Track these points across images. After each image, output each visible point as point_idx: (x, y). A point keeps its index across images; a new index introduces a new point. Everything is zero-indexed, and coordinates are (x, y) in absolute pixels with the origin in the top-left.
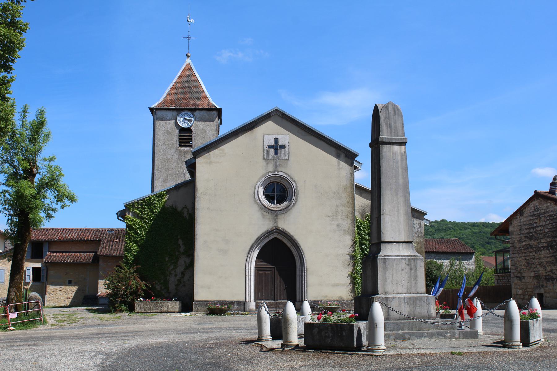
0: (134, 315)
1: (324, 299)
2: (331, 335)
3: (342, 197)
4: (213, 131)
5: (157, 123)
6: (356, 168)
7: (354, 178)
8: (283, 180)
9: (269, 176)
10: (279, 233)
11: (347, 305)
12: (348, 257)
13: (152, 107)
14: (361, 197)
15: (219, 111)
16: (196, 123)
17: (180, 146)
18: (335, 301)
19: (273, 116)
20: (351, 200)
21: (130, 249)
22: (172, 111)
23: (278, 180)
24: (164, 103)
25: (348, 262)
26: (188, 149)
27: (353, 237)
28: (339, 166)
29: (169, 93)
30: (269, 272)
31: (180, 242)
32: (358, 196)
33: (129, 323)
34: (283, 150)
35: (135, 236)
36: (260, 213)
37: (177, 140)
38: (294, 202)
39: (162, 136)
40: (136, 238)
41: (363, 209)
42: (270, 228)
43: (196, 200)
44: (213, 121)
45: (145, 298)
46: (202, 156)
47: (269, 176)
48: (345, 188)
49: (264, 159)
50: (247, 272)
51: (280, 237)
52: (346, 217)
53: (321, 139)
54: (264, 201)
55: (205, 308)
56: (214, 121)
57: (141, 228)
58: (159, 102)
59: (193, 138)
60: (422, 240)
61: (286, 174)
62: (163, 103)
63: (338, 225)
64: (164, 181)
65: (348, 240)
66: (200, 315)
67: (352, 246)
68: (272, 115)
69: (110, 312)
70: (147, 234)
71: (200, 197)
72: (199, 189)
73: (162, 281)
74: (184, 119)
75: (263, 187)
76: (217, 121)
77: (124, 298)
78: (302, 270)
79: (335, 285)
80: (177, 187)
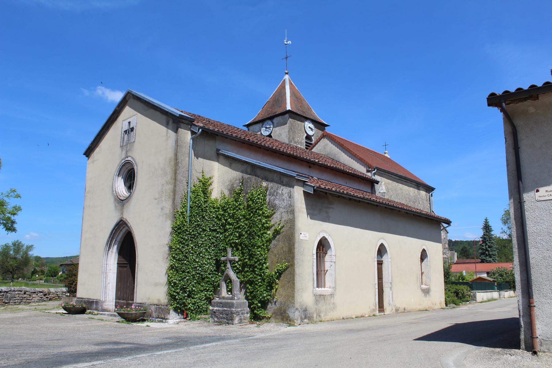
1: (148, 302)
3: (167, 173)
4: (286, 133)
9: (122, 163)
11: (163, 310)
12: (167, 248)
18: (154, 305)
19: (129, 99)
20: (173, 175)
25: (167, 255)
27: (172, 221)
28: (167, 135)
32: (227, 168)
34: (132, 133)
41: (232, 183)
46: (90, 157)
47: (122, 163)
49: (121, 146)
52: (169, 197)
54: (120, 191)
56: (286, 124)
61: (132, 158)
63: (162, 209)
65: (168, 227)
67: (171, 234)
71: (86, 196)
75: (121, 176)
79: (156, 285)
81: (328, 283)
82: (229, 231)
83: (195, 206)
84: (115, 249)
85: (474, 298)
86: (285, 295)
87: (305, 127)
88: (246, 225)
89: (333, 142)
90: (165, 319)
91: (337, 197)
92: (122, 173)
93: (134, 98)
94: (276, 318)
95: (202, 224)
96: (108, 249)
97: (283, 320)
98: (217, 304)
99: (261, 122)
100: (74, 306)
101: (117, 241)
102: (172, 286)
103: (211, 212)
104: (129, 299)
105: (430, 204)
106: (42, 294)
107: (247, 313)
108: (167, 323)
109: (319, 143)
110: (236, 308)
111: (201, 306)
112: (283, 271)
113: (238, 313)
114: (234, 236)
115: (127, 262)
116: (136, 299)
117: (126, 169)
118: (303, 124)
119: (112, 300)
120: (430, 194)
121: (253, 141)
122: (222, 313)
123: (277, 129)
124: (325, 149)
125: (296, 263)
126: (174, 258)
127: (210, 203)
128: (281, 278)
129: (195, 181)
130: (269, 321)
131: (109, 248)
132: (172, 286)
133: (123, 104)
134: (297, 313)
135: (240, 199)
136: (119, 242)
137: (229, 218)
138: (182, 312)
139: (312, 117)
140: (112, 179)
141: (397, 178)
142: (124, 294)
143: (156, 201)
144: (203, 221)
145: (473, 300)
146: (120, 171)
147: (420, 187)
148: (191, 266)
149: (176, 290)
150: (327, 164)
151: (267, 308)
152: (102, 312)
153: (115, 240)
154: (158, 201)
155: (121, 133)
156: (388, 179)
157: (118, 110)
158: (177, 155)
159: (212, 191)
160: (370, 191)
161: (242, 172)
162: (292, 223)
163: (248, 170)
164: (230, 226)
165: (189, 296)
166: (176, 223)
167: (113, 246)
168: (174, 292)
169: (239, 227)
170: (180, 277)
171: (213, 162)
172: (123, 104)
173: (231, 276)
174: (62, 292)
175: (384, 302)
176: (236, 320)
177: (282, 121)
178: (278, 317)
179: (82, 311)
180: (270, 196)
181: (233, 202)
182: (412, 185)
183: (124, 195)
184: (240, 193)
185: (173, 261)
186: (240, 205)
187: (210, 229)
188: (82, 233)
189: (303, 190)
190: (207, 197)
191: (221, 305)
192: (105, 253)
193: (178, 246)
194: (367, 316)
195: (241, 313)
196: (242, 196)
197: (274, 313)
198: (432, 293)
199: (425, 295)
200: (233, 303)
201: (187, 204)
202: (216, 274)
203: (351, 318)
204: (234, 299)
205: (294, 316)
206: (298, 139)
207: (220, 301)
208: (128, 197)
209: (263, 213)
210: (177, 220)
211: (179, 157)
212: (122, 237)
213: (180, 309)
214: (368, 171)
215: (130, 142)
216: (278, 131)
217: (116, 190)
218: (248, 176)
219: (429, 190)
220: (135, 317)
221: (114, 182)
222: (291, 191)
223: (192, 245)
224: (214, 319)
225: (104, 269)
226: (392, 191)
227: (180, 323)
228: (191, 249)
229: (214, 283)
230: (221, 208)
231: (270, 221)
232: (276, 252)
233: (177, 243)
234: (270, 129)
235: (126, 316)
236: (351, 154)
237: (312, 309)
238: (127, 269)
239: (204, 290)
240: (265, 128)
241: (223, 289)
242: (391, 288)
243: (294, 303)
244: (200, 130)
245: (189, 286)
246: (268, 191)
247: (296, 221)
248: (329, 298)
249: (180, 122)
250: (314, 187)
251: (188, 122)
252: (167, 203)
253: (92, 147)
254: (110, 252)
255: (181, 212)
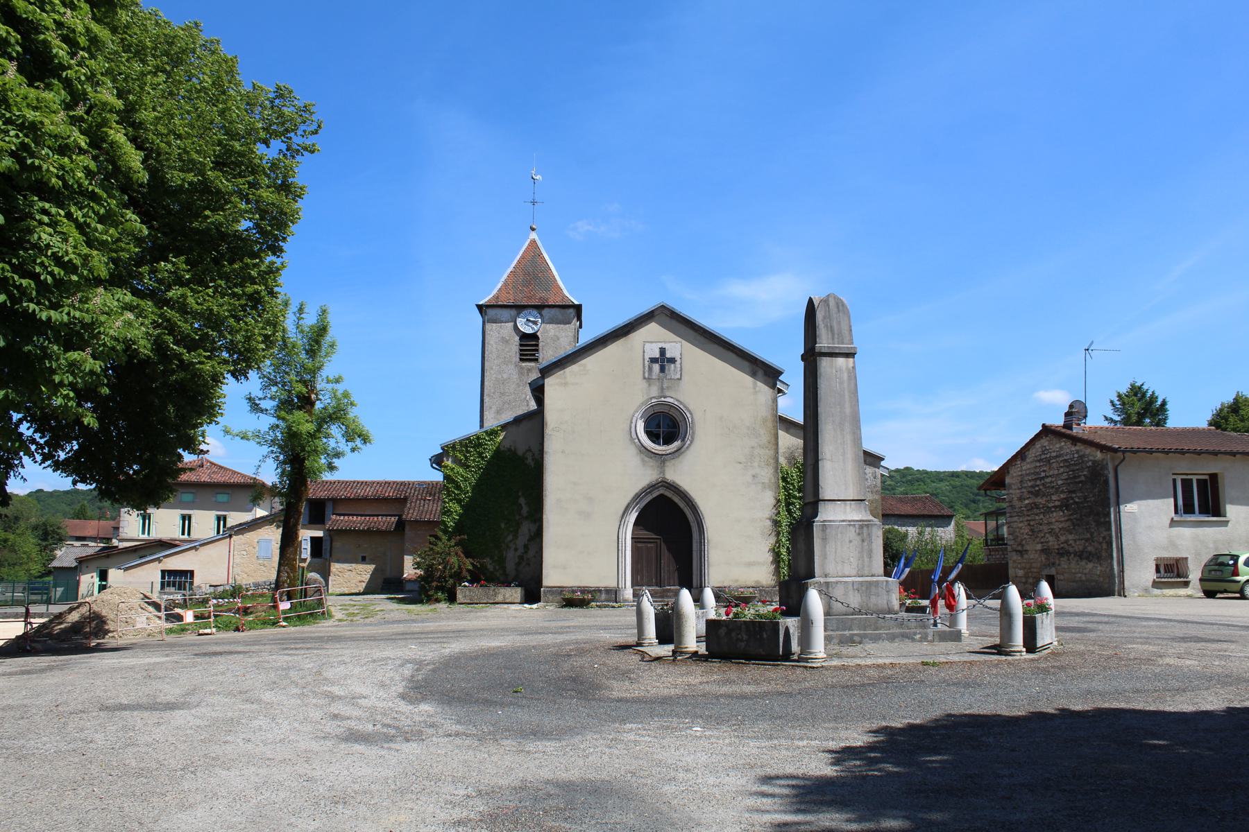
0: (455, 607)
1: (734, 585)
2: (745, 637)
5: (488, 326)
6: (780, 391)
7: (777, 405)
8: (672, 410)
10: (667, 488)
11: (767, 593)
12: (769, 523)
13: (481, 303)
15: (578, 309)
17: (521, 360)
21: (449, 511)
23: (666, 410)
24: (497, 298)
26: (532, 364)
28: (755, 388)
29: (506, 284)
30: (652, 545)
31: (522, 501)
33: (449, 619)
34: (673, 365)
35: (456, 492)
37: (518, 351)
38: (689, 442)
39: (494, 346)
40: (458, 495)
42: (654, 479)
43: (545, 439)
44: (569, 323)
45: (472, 582)
48: (764, 421)
49: (644, 378)
50: (620, 545)
51: (668, 494)
53: (729, 349)
55: (559, 598)
57: (466, 481)
58: (491, 296)
59: (540, 347)
60: (877, 497)
61: (677, 400)
62: (497, 297)
63: (754, 476)
64: (498, 412)
65: (769, 498)
66: (551, 608)
68: (656, 313)
69: (421, 602)
70: (474, 488)
72: (549, 424)
73: (496, 558)
74: (527, 320)
76: (576, 323)
77: (441, 582)
78: (701, 542)
79: (750, 564)
80: (518, 420)
84: (633, 517)
140: (629, 422)
177: (560, 317)
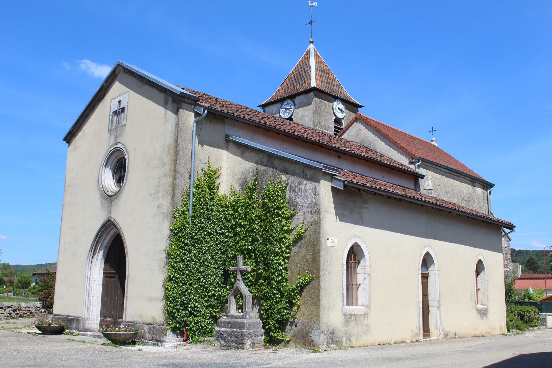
1: (140, 320)
3: (165, 163)
9: (110, 152)
11: (158, 330)
12: (164, 255)
14: (243, 158)
16: (296, 111)
18: (148, 324)
19: (119, 73)
20: (173, 166)
22: (277, 104)
27: (171, 222)
28: (165, 117)
32: (240, 158)
34: (123, 114)
36: (100, 202)
41: (244, 177)
47: (110, 152)
49: (109, 131)
52: (167, 192)
56: (311, 104)
61: (123, 145)
63: (159, 207)
67: (169, 237)
71: (66, 190)
75: (109, 167)
79: (150, 299)
81: (360, 301)
82: (239, 235)
83: (199, 204)
84: (100, 255)
85: (544, 322)
86: (308, 314)
87: (334, 108)
88: (261, 227)
89: (368, 127)
90: (161, 342)
91: (372, 194)
92: (109, 163)
93: (125, 72)
94: (296, 342)
95: (208, 226)
96: (92, 255)
97: (305, 345)
98: (224, 324)
99: (280, 101)
100: (49, 325)
101: (103, 246)
102: (170, 301)
103: (218, 211)
104: (117, 317)
105: (488, 204)
106: (10, 309)
107: (261, 336)
108: (163, 347)
109: (351, 128)
110: (247, 329)
111: (205, 326)
112: (306, 285)
113: (250, 336)
114: (246, 241)
115: (115, 271)
116: (125, 317)
117: (115, 158)
118: (331, 104)
119: (96, 317)
120: (488, 191)
121: (270, 125)
122: (230, 335)
123: (299, 110)
124: (358, 135)
125: (321, 275)
126: (173, 267)
127: (217, 200)
128: (303, 293)
129: (199, 173)
130: (288, 345)
131: (94, 254)
132: (170, 301)
133: (111, 78)
134: (322, 337)
135: (254, 196)
136: (106, 247)
137: (240, 219)
138: (182, 334)
139: (342, 96)
141: (447, 171)
142: (111, 311)
143: (152, 197)
144: (208, 222)
145: (543, 325)
146: (107, 161)
147: (475, 182)
148: (194, 277)
149: (175, 306)
150: (361, 154)
151: (285, 329)
152: (84, 333)
153: (101, 244)
154: (154, 198)
155: (109, 114)
156: (436, 173)
157: (105, 86)
158: (177, 141)
159: (219, 186)
160: (413, 188)
161: (256, 163)
162: (317, 225)
163: (264, 160)
164: (241, 229)
165: (191, 314)
166: (176, 224)
167: (99, 251)
168: (174, 308)
169: (252, 231)
170: (181, 290)
171: (221, 150)
172: (111, 78)
173: (242, 289)
174: (35, 307)
175: (430, 325)
176: (248, 344)
177: (305, 101)
178: (299, 341)
179: (60, 331)
180: (291, 192)
181: (245, 199)
182: (466, 180)
183: (112, 190)
184: (255, 189)
185: (172, 271)
186: (254, 203)
187: (216, 232)
188: (60, 236)
189: (331, 186)
190: (213, 193)
191: (230, 325)
192: (88, 260)
193: (178, 252)
194: (408, 341)
195: (253, 335)
196: (256, 191)
197: (294, 336)
198: (490, 315)
199: (482, 318)
200: (244, 322)
201: (189, 202)
202: (224, 287)
203: (388, 344)
204: (246, 318)
205: (319, 339)
206: (325, 122)
207: (228, 320)
208: (118, 192)
209: (283, 213)
210: (176, 220)
211: (180, 144)
212: (109, 241)
213: (179, 329)
214: (411, 163)
215: (120, 125)
216: (301, 113)
217: (103, 184)
218: (263, 168)
219: (487, 187)
220: (124, 339)
221: (100, 174)
222: (316, 187)
223: (195, 252)
224: (220, 342)
225: (86, 279)
226: (440, 188)
227: (178, 347)
228: (193, 256)
229: (220, 298)
230: (231, 207)
231: (290, 223)
232: (297, 261)
233: (177, 248)
234: (291, 111)
235: (113, 337)
236: (390, 141)
237: (340, 332)
238: (115, 280)
239: (209, 305)
240: (284, 110)
241: (232, 305)
242: (438, 307)
243: (318, 324)
244: (206, 111)
245: (191, 301)
246: (288, 186)
247: (322, 223)
248: (362, 318)
249: (181, 101)
250: (344, 181)
251: (191, 101)
252: (164, 199)
253: (74, 131)
254: (94, 259)
255: (182, 211)
